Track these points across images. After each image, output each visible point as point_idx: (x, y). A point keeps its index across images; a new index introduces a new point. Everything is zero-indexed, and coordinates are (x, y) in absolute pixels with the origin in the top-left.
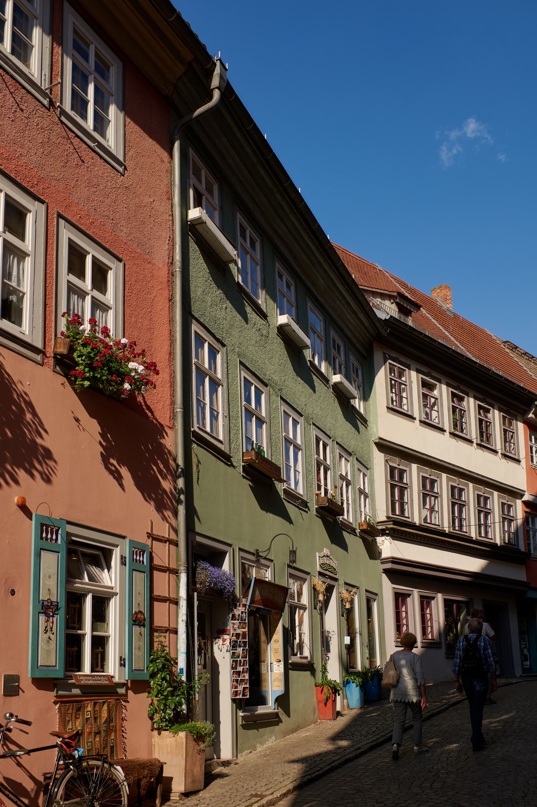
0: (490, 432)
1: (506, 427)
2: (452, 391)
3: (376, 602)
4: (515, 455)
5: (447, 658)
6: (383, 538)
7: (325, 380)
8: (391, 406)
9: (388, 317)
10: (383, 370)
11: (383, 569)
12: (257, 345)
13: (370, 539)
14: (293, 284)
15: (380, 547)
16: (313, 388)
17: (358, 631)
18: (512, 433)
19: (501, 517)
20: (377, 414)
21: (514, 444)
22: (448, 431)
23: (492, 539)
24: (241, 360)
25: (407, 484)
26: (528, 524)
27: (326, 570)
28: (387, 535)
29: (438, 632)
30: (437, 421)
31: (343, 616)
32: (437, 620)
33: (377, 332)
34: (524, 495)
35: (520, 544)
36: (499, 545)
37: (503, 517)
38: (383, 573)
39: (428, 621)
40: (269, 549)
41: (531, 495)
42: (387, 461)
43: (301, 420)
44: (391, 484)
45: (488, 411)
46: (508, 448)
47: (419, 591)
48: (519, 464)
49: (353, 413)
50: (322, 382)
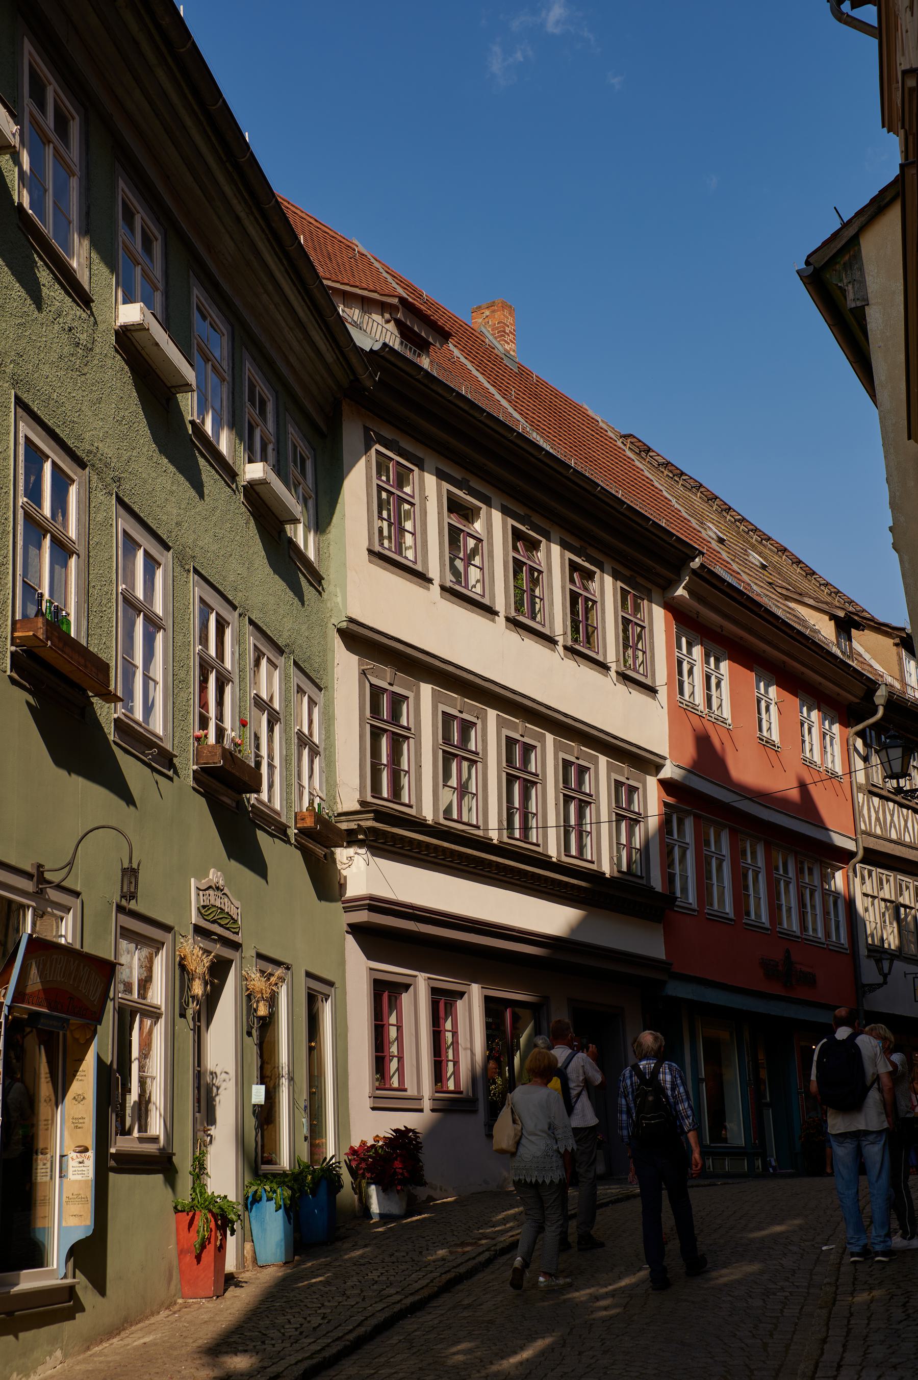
0: (593, 623)
2: (513, 527)
3: (329, 1001)
4: (646, 676)
6: (351, 851)
7: (229, 473)
8: (377, 548)
9: (377, 347)
10: (362, 463)
11: (349, 925)
12: (62, 364)
13: (320, 851)
14: (159, 237)
15: (344, 873)
16: (198, 487)
17: (285, 1071)
18: (639, 629)
20: (345, 564)
21: (644, 653)
22: (502, 614)
23: (593, 862)
24: (19, 394)
25: (410, 729)
26: (670, 833)
27: (214, 922)
28: (361, 844)
29: (470, 1074)
30: (478, 589)
31: (249, 1034)
32: (469, 1046)
33: (352, 378)
35: (652, 875)
36: (607, 876)
38: (347, 932)
39: (449, 1048)
40: (71, 864)
41: (678, 766)
42: (365, 674)
43: (165, 559)
44: (372, 726)
45: (590, 576)
46: (630, 661)
47: (429, 978)
48: (654, 698)
49: (290, 557)
50: (220, 475)
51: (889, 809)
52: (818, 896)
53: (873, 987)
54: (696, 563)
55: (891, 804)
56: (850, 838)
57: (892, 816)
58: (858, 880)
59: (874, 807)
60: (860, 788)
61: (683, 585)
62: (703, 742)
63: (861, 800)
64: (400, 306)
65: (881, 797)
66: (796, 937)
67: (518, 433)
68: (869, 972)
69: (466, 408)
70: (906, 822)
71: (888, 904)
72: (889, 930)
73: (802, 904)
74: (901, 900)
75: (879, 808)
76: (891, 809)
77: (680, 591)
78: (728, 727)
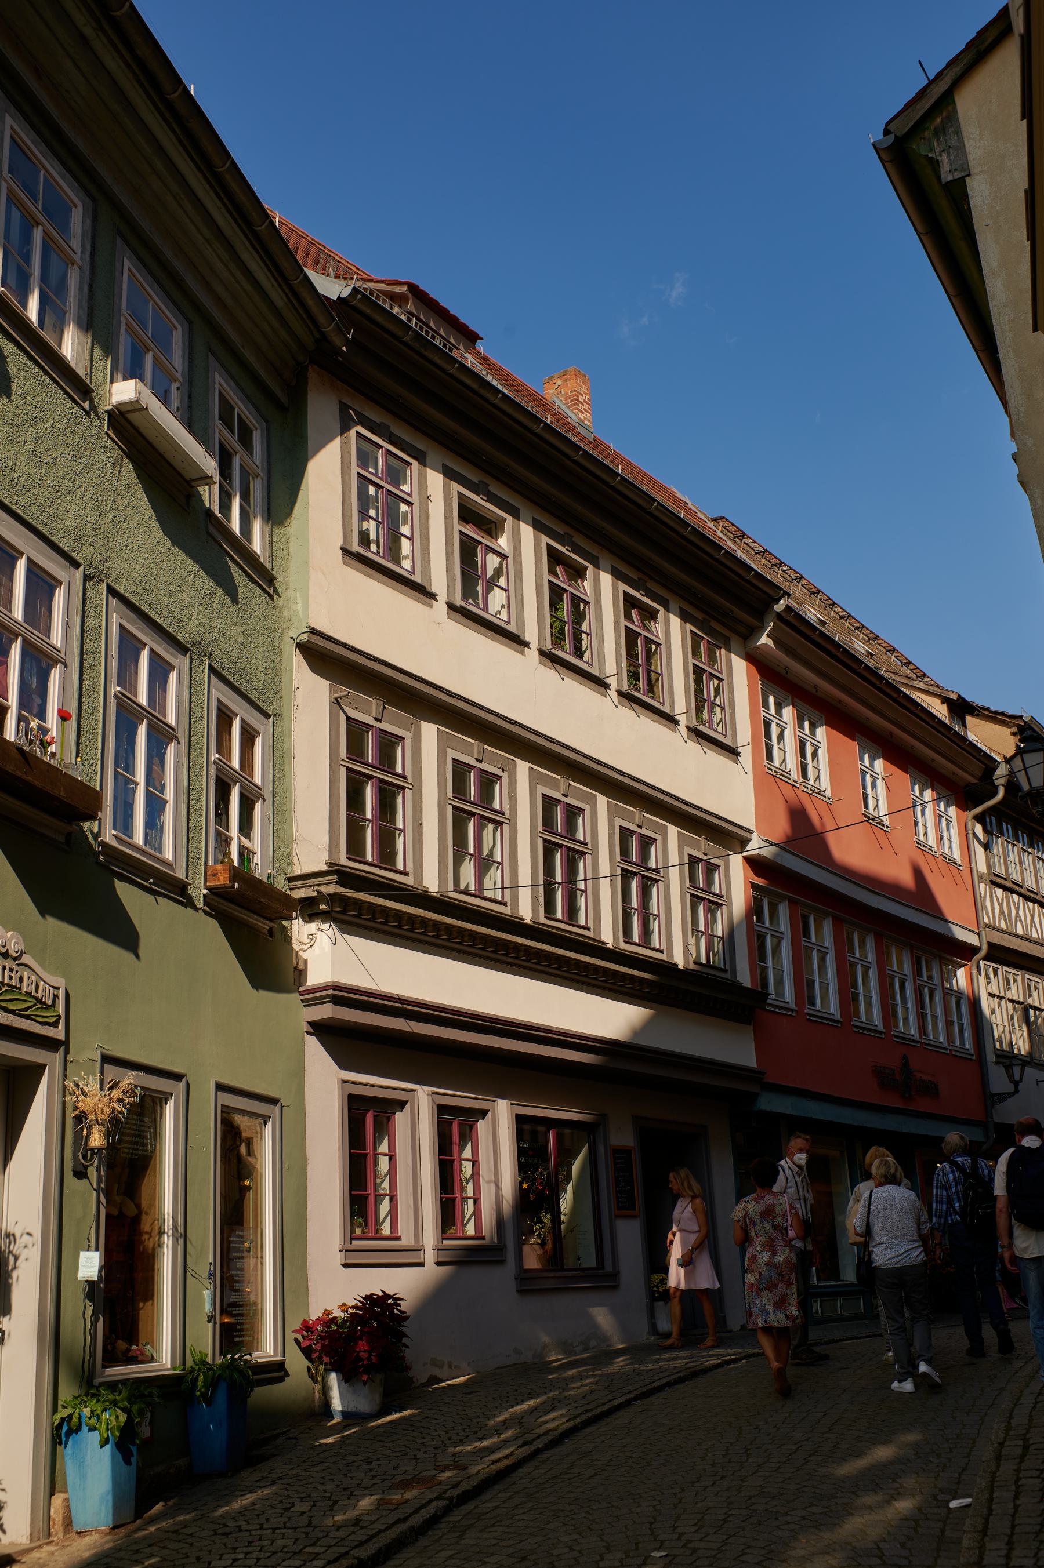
0: (657, 669)
1: (701, 662)
2: (548, 544)
3: (270, 1125)
4: (726, 736)
5: (520, 1292)
6: (312, 927)
11: (310, 1023)
15: (304, 955)
17: (168, 1225)
18: (716, 682)
19: (688, 895)
20: (307, 562)
21: (723, 708)
22: (534, 645)
23: (661, 951)
25: (405, 778)
26: (760, 919)
28: (324, 916)
29: (494, 1214)
30: (504, 615)
32: (493, 1178)
33: (317, 336)
34: (748, 841)
35: (738, 968)
36: (681, 967)
37: (692, 895)
38: (308, 1033)
39: (468, 1182)
41: (766, 841)
42: (339, 704)
45: (653, 615)
46: (705, 716)
47: (433, 1093)
48: (736, 761)
49: (209, 534)
51: (1014, 902)
52: (938, 996)
53: (1003, 1097)
54: (780, 606)
55: (1016, 897)
56: (972, 931)
57: (1017, 909)
58: (982, 979)
59: (998, 899)
60: (981, 877)
61: (767, 632)
62: (798, 816)
63: (983, 892)
64: (410, 295)
65: (1005, 888)
66: (914, 1041)
67: (546, 424)
68: (998, 1081)
69: (475, 386)
70: (1032, 916)
71: (1017, 1005)
72: (1018, 1033)
73: (920, 1004)
74: (1030, 1001)
75: (1002, 900)
76: (1016, 901)
77: (764, 640)
78: (827, 800)
